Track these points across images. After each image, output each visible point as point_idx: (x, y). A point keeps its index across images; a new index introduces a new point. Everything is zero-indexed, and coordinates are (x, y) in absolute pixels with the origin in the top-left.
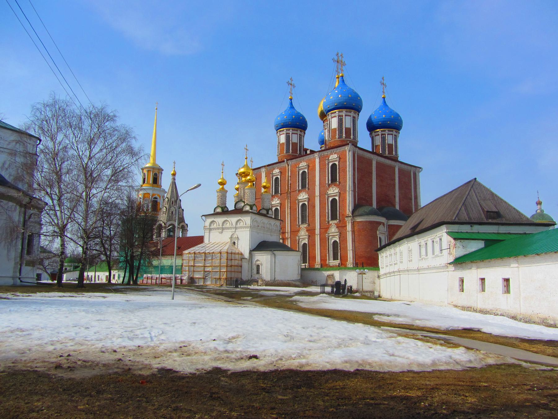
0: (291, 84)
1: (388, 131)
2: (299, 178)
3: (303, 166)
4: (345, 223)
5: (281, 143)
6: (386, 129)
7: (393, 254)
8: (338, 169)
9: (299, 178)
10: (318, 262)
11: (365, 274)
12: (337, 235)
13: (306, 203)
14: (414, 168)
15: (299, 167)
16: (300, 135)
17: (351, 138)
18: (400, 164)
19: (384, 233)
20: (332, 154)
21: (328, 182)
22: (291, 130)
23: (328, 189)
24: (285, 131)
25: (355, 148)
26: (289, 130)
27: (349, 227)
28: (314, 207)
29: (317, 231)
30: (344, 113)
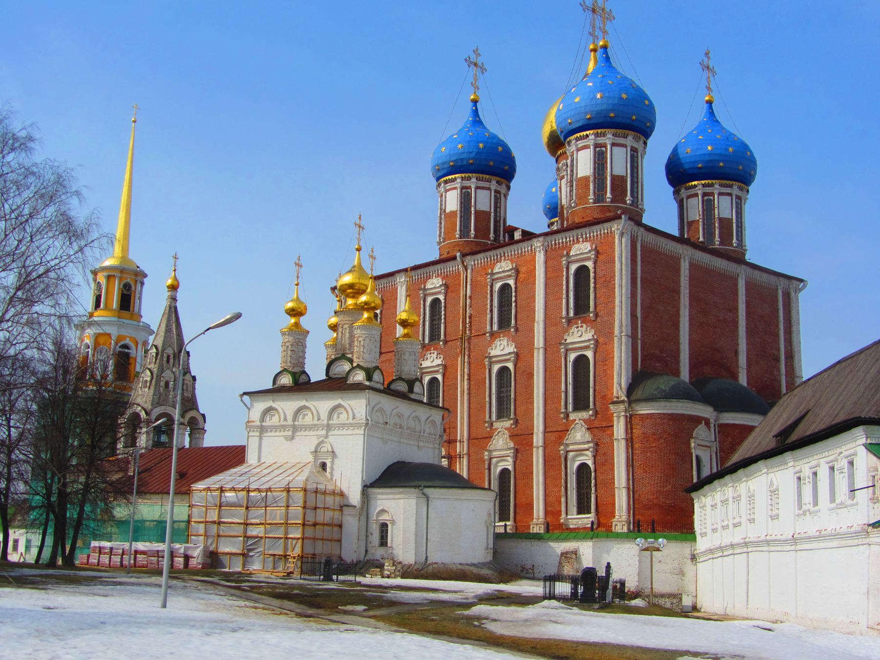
0: (476, 65)
1: (721, 185)
2: (492, 301)
3: (504, 272)
4: (610, 419)
5: (448, 211)
6: (714, 181)
7: (731, 500)
8: (592, 281)
9: (492, 301)
10: (538, 519)
11: (658, 550)
12: (588, 450)
13: (510, 365)
14: (786, 281)
15: (492, 274)
16: (496, 191)
17: (625, 203)
18: (749, 270)
19: (708, 444)
20: (578, 242)
21: (568, 313)
22: (474, 180)
23: (566, 331)
24: (459, 180)
25: (636, 228)
26: (469, 179)
27: (619, 429)
28: (530, 375)
29: (538, 439)
30: (608, 138)
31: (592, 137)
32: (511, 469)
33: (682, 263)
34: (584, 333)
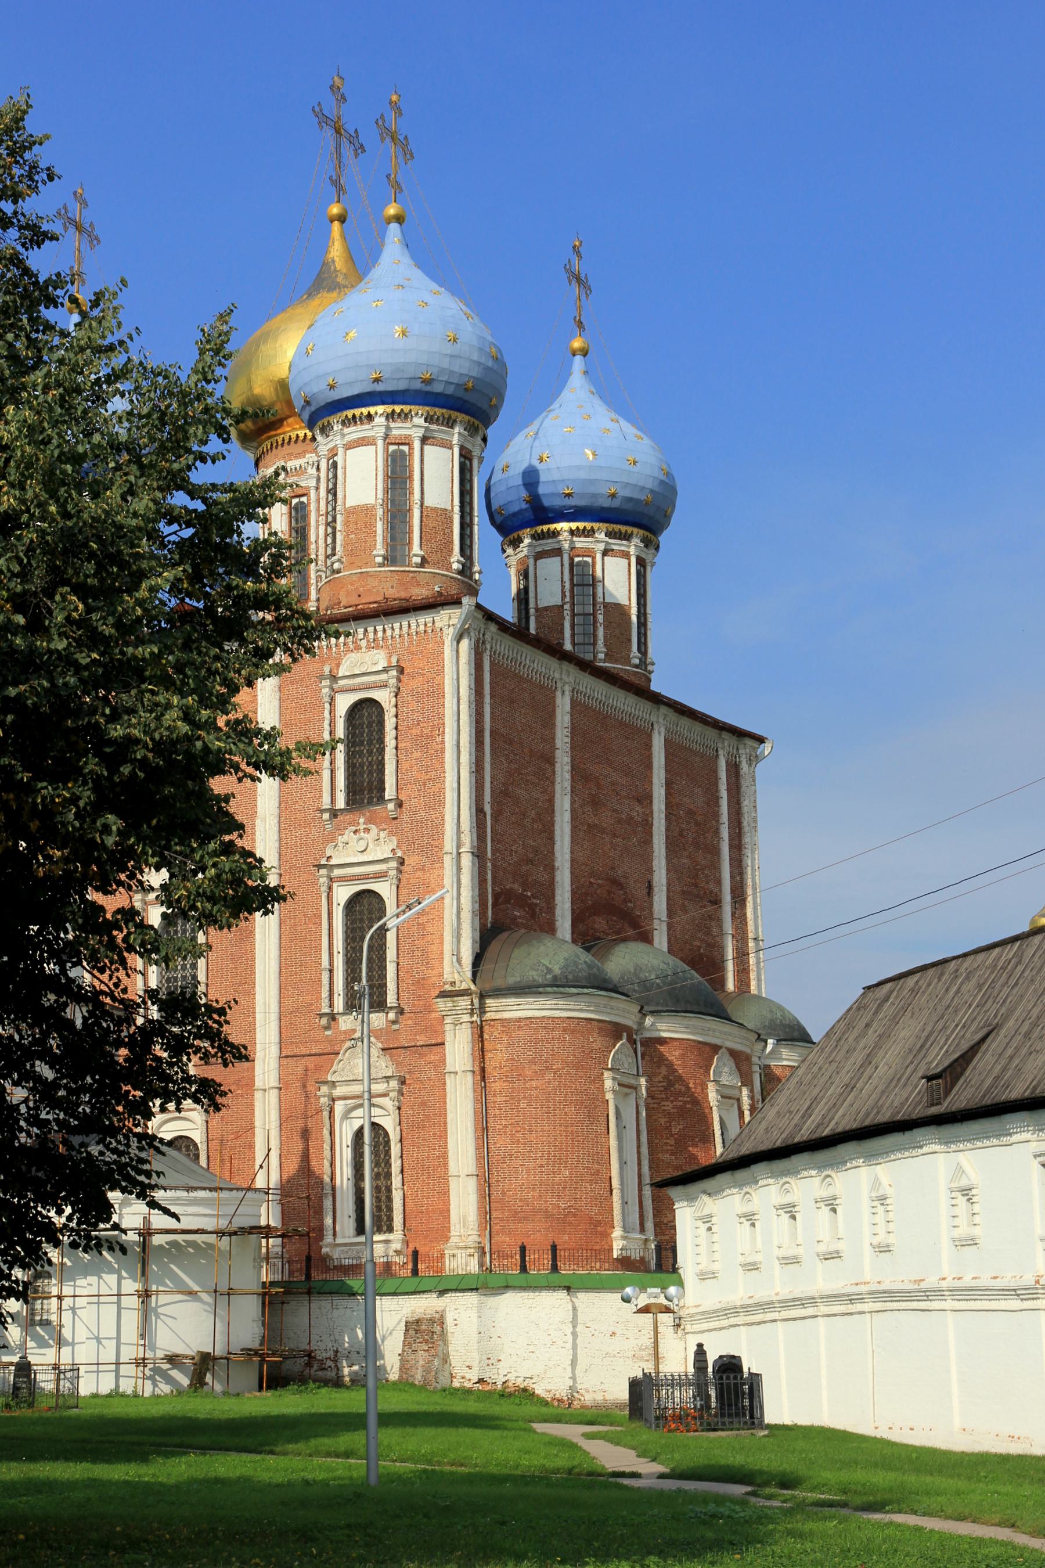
1: (608, 534)
6: (596, 525)
12: (386, 1095)
17: (449, 568)
20: (358, 648)
21: (333, 800)
30: (414, 427)
31: (380, 420)
32: (198, 1140)
33: (559, 700)
34: (371, 846)
